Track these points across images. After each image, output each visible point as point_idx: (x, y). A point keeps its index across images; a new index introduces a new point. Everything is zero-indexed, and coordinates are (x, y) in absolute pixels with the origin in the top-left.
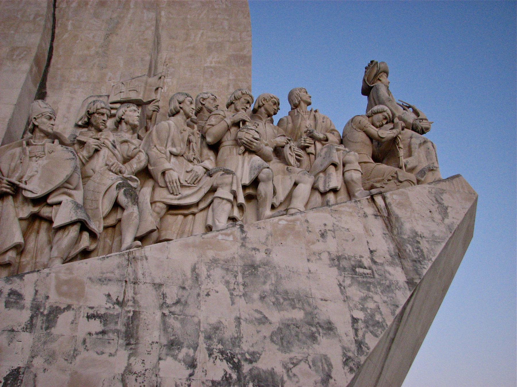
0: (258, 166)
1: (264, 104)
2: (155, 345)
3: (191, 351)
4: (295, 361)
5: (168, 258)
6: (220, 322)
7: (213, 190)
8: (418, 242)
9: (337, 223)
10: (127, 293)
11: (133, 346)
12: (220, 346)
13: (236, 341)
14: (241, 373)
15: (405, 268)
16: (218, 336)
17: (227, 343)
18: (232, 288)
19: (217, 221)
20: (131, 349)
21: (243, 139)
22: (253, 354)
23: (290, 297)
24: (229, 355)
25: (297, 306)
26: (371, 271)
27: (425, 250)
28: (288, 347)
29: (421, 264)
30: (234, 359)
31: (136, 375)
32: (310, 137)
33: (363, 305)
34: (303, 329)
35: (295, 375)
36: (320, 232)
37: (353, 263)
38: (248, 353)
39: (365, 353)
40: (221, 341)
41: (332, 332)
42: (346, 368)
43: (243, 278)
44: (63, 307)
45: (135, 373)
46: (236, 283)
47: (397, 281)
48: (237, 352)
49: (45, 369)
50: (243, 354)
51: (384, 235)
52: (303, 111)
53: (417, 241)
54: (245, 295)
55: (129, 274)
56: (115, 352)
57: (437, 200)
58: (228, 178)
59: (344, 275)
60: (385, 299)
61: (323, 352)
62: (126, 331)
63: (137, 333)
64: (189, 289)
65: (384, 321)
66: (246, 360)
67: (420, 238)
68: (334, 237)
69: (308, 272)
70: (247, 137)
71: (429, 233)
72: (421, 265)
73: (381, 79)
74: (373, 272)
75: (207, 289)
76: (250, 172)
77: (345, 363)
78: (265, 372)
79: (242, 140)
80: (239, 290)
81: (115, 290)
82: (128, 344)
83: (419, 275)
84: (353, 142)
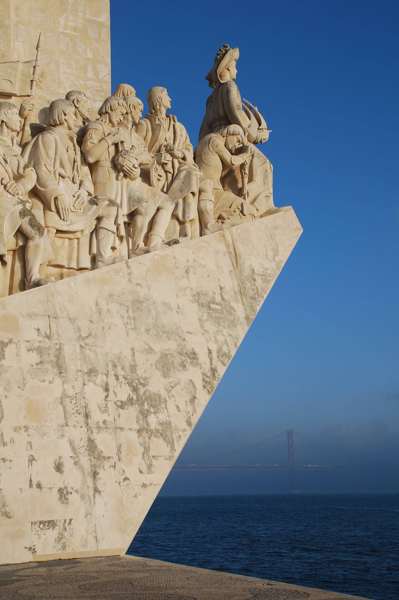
0: (138, 199)
1: (131, 112)
2: (79, 373)
3: (105, 377)
4: (173, 385)
5: (76, 293)
6: (121, 352)
7: (99, 219)
8: (255, 280)
9: (196, 259)
10: (51, 327)
11: (64, 374)
12: (123, 373)
13: (133, 368)
14: (138, 394)
15: (245, 304)
16: (121, 364)
17: (128, 370)
18: (126, 322)
19: (103, 251)
20: (63, 377)
21: (123, 166)
22: (145, 379)
23: (167, 330)
24: (130, 380)
25: (172, 338)
26: (221, 307)
27: (259, 288)
28: (167, 373)
29: (256, 301)
30: (133, 383)
31: (70, 398)
32: (170, 154)
33: (215, 338)
34: (177, 358)
35: (173, 396)
36: (185, 268)
37: (209, 299)
38: (142, 379)
39: (217, 379)
40: (123, 368)
41: (195, 361)
42: (205, 390)
43: (133, 314)
44: (6, 341)
45: (69, 397)
46: (128, 317)
47: (238, 317)
48: (135, 377)
49: (6, 396)
50: (138, 379)
51: (230, 272)
52: (163, 119)
53: (254, 278)
54: (135, 328)
55: (50, 310)
56: (53, 380)
57: (271, 236)
58: (113, 210)
59: (202, 310)
60: (230, 332)
61: (191, 378)
62: (57, 362)
63: (65, 362)
64: (96, 323)
65: (229, 352)
66: (141, 384)
67: (256, 275)
68: (195, 274)
69: (178, 307)
70: (129, 166)
71: (263, 270)
72: (255, 302)
73: (230, 69)
74: (222, 308)
75: (108, 323)
76: (129, 202)
77: (204, 387)
78: (154, 394)
79: (124, 168)
80: (131, 324)
81: (42, 324)
82: (60, 373)
83: (254, 311)
84: (207, 165)
